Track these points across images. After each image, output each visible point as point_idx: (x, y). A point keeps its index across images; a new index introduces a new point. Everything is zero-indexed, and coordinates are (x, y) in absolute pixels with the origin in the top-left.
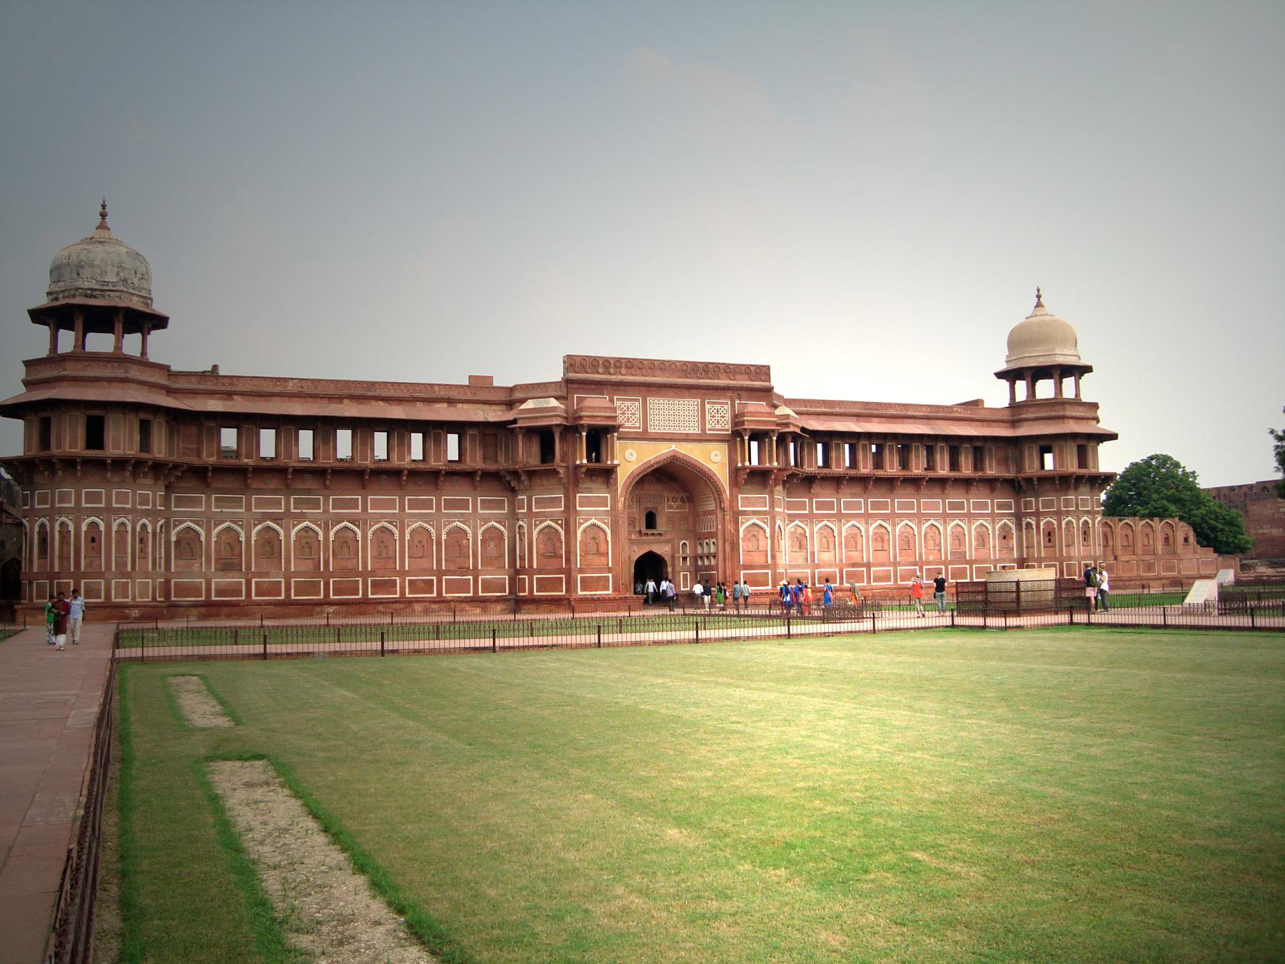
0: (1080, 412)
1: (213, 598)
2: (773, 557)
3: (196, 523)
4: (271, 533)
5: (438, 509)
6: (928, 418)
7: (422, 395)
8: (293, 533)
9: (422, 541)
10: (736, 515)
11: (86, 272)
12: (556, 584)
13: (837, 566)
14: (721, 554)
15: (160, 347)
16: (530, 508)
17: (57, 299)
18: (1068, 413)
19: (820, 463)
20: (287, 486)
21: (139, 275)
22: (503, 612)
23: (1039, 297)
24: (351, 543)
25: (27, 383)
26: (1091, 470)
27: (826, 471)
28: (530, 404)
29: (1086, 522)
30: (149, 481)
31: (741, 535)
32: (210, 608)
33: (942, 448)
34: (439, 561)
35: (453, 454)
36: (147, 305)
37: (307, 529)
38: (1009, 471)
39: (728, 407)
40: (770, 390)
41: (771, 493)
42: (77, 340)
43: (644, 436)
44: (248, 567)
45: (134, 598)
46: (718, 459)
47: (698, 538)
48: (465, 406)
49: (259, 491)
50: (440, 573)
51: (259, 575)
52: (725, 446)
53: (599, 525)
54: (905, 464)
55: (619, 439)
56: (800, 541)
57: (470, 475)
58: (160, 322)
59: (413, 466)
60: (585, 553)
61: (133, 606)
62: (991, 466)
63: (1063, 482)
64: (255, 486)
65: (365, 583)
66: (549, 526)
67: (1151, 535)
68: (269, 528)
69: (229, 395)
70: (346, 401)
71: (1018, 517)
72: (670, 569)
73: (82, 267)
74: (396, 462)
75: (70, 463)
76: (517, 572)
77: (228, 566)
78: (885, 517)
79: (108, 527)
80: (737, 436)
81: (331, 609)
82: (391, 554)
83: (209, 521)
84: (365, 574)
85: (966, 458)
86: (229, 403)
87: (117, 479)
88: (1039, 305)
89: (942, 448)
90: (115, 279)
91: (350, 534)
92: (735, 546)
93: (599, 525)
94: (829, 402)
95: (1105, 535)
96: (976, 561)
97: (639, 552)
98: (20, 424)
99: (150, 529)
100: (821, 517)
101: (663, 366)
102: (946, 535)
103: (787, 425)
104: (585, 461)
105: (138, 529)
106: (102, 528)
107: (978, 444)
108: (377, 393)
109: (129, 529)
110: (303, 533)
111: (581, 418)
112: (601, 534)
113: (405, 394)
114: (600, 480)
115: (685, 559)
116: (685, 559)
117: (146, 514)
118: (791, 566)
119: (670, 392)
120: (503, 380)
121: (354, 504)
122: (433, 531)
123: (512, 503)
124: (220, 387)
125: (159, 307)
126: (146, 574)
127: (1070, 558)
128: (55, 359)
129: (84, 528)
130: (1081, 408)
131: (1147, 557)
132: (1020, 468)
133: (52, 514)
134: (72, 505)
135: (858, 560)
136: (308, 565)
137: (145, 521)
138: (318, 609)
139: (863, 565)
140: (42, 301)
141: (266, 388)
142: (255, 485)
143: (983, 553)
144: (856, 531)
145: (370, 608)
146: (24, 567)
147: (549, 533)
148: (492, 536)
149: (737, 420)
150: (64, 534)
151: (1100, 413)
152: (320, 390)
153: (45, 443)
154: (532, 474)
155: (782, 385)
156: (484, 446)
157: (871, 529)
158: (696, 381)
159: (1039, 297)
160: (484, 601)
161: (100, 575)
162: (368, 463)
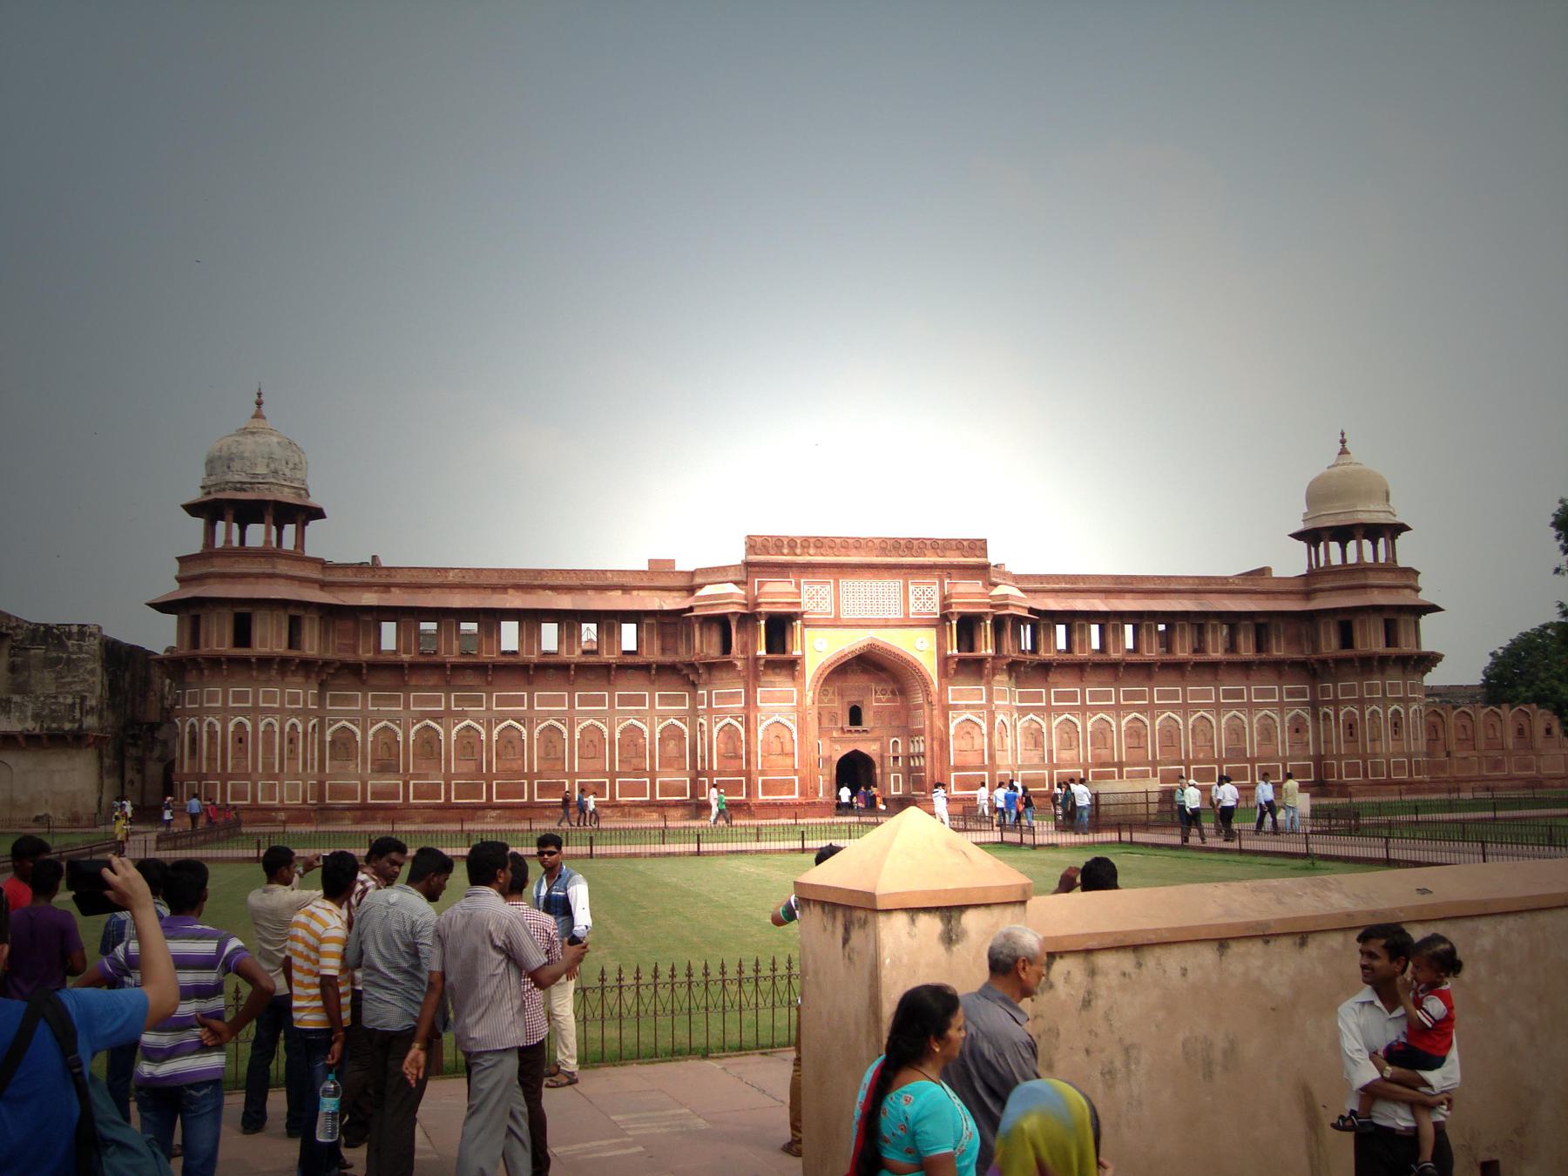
0: (1388, 579)
2: (992, 757)
3: (351, 721)
5: (612, 705)
7: (594, 583)
9: (593, 741)
10: (946, 709)
11: (236, 465)
13: (1080, 765)
14: (928, 754)
15: (321, 541)
16: (710, 703)
18: (1371, 581)
20: (448, 683)
22: (683, 818)
23: (1343, 442)
24: (516, 742)
25: (182, 580)
26: (1406, 648)
29: (1397, 712)
30: (299, 679)
31: (952, 732)
33: (1182, 628)
37: (469, 727)
38: (1302, 652)
39: (936, 588)
41: (989, 683)
43: (836, 623)
44: (406, 768)
45: (282, 801)
47: (911, 734)
48: (642, 593)
49: (417, 688)
50: (613, 775)
51: (417, 776)
52: (932, 632)
53: (786, 725)
56: (1036, 738)
57: (645, 668)
58: (318, 514)
59: (583, 659)
60: (768, 753)
64: (413, 682)
67: (1498, 726)
68: (428, 726)
69: (387, 587)
70: (511, 591)
71: (1314, 706)
72: (878, 771)
73: (231, 459)
74: (565, 656)
75: (215, 662)
76: (699, 774)
77: (385, 766)
79: (255, 727)
81: (494, 813)
83: (365, 720)
84: (531, 776)
85: (1246, 637)
87: (263, 677)
88: (1344, 452)
92: (944, 745)
93: (786, 725)
96: (1259, 759)
97: (841, 751)
98: (172, 619)
99: (300, 729)
100: (1095, 710)
101: (846, 544)
102: (1219, 728)
103: (1006, 606)
104: (762, 652)
105: (287, 729)
106: (249, 728)
107: (1261, 621)
108: (545, 581)
109: (277, 729)
110: (464, 733)
111: (758, 605)
113: (575, 582)
114: (784, 672)
115: (896, 759)
116: (896, 759)
117: (296, 713)
118: (1020, 768)
119: (867, 572)
123: (693, 698)
125: (315, 500)
126: (296, 776)
127: (1375, 755)
129: (231, 728)
130: (1389, 575)
131: (1491, 753)
132: (1316, 649)
133: (200, 713)
136: (470, 767)
137: (294, 720)
138: (480, 813)
139: (1114, 765)
140: (196, 495)
145: (536, 811)
146: (177, 769)
147: (729, 732)
148: (672, 734)
149: (945, 604)
152: (483, 580)
153: (195, 643)
154: (711, 667)
156: (663, 636)
157: (1123, 723)
158: (901, 559)
159: (1343, 442)
160: (662, 806)
161: (247, 776)
162: (535, 658)
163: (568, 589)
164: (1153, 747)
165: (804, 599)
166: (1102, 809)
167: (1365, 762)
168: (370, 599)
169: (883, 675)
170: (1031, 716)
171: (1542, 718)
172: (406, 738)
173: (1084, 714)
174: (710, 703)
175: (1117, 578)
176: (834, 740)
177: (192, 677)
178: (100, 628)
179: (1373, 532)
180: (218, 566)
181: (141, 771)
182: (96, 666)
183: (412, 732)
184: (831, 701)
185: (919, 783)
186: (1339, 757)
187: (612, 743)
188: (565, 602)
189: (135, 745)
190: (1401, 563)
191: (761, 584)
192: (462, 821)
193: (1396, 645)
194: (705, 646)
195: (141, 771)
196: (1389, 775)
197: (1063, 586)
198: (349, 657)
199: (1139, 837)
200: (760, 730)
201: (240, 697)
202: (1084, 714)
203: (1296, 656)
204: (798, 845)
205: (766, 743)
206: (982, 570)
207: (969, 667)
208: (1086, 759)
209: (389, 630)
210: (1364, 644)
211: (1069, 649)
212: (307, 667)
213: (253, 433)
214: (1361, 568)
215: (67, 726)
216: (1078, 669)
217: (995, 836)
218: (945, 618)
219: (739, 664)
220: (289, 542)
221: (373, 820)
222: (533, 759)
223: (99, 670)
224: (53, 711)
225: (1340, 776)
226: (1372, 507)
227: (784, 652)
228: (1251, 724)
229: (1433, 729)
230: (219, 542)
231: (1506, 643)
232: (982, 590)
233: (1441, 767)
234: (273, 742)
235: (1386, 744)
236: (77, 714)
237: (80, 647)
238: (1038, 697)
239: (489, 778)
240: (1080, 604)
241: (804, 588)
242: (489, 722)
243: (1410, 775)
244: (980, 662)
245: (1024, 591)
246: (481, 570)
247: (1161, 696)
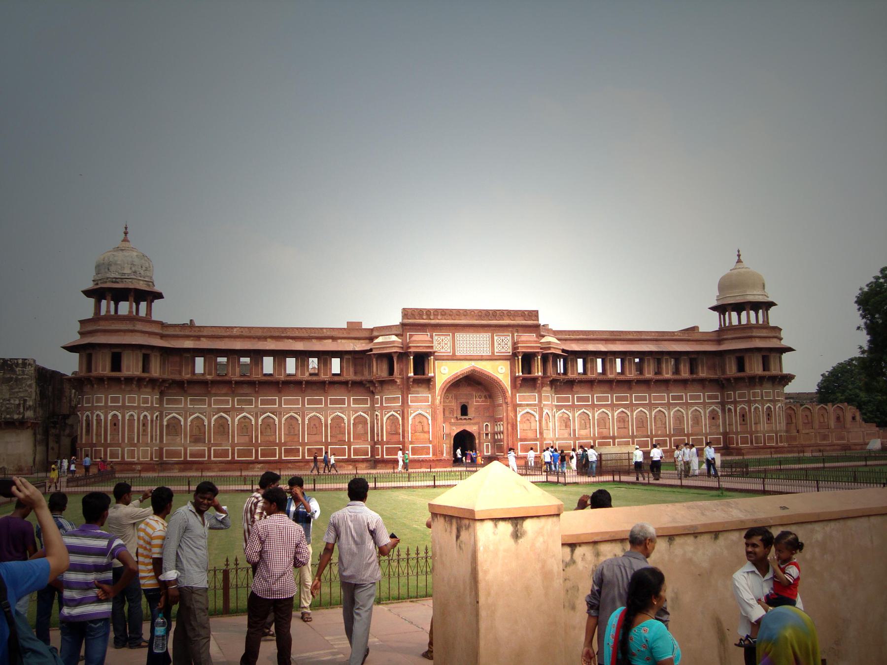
0: (764, 333)
1: (188, 459)
2: (541, 433)
3: (178, 414)
6: (656, 340)
7: (316, 335)
8: (236, 420)
10: (515, 406)
11: (113, 268)
13: (591, 438)
14: (505, 432)
15: (161, 311)
16: (382, 403)
18: (754, 334)
20: (233, 392)
22: (367, 468)
23: (739, 256)
25: (81, 333)
26: (774, 371)
27: (584, 377)
29: (769, 408)
30: (149, 390)
31: (519, 419)
33: (649, 360)
34: (326, 436)
36: (149, 285)
37: (245, 417)
38: (716, 374)
39: (509, 338)
40: (537, 326)
43: (453, 358)
44: (210, 440)
45: (138, 459)
46: (503, 371)
48: (343, 341)
49: (216, 395)
50: (327, 444)
51: (215, 445)
52: (508, 363)
53: (425, 416)
55: (435, 359)
56: (566, 422)
57: (345, 383)
58: (159, 296)
59: (310, 378)
60: (415, 431)
61: (136, 464)
62: (703, 370)
64: (213, 392)
67: (826, 416)
68: (221, 416)
69: (198, 338)
70: (269, 340)
71: (723, 404)
72: (477, 441)
74: (300, 377)
75: (101, 380)
76: (375, 443)
77: (197, 439)
78: (625, 406)
81: (260, 466)
82: (296, 432)
83: (186, 413)
84: (280, 445)
85: (685, 366)
87: (128, 389)
88: (739, 261)
89: (667, 360)
90: (129, 272)
92: (514, 426)
93: (425, 416)
96: (692, 435)
97: (456, 430)
98: (76, 356)
99: (149, 418)
101: (459, 313)
103: (549, 348)
104: (411, 374)
105: (142, 418)
106: (120, 418)
108: (289, 334)
109: (136, 418)
111: (410, 347)
112: (425, 419)
115: (487, 434)
116: (487, 434)
117: (147, 409)
118: (557, 439)
121: (273, 402)
124: (192, 333)
125: (157, 288)
126: (147, 445)
127: (757, 432)
128: (97, 318)
130: (764, 331)
131: (822, 431)
132: (723, 371)
133: (92, 409)
134: (103, 404)
137: (145, 413)
138: (251, 466)
139: (610, 438)
140: (90, 285)
144: (605, 415)
146: (79, 441)
148: (360, 421)
150: (99, 421)
151: (783, 334)
152: (253, 334)
153: (89, 369)
154: (382, 383)
156: (355, 365)
157: (616, 414)
159: (739, 256)
160: (355, 461)
161: (119, 445)
162: (282, 377)
164: (632, 428)
165: (435, 344)
166: (604, 463)
167: (751, 436)
168: (189, 344)
169: (480, 387)
170: (563, 410)
171: (850, 411)
172: (209, 423)
174: (382, 403)
175: (612, 332)
176: (452, 424)
177: (87, 388)
178: (34, 361)
179: (756, 306)
180: (103, 325)
181: (58, 441)
182: (33, 382)
184: (450, 402)
185: (500, 448)
186: (737, 433)
188: (299, 346)
189: (55, 427)
190: (772, 323)
191: (411, 336)
192: (241, 470)
193: (768, 370)
195: (58, 441)
196: (765, 443)
197: (581, 337)
198: (177, 377)
199: (624, 478)
200: (410, 418)
201: (115, 400)
204: (432, 483)
207: (528, 383)
208: (594, 434)
209: (199, 362)
210: (751, 369)
211: (585, 372)
212: (153, 383)
213: (122, 250)
214: (749, 327)
215: (16, 417)
216: (591, 384)
217: (543, 478)
218: (515, 355)
220: (143, 312)
221: (190, 469)
222: (282, 436)
223: (34, 385)
224: (8, 408)
225: (737, 444)
226: (755, 293)
227: (424, 374)
228: (687, 414)
229: (790, 419)
230: (103, 312)
231: (830, 369)
232: (536, 339)
233: (795, 438)
235: (763, 426)
236: (22, 410)
237: (23, 371)
238: (567, 400)
239: (257, 445)
240: (591, 347)
241: (435, 338)
242: (257, 414)
243: (777, 443)
244: (535, 380)
245: (559, 340)
246: (253, 328)
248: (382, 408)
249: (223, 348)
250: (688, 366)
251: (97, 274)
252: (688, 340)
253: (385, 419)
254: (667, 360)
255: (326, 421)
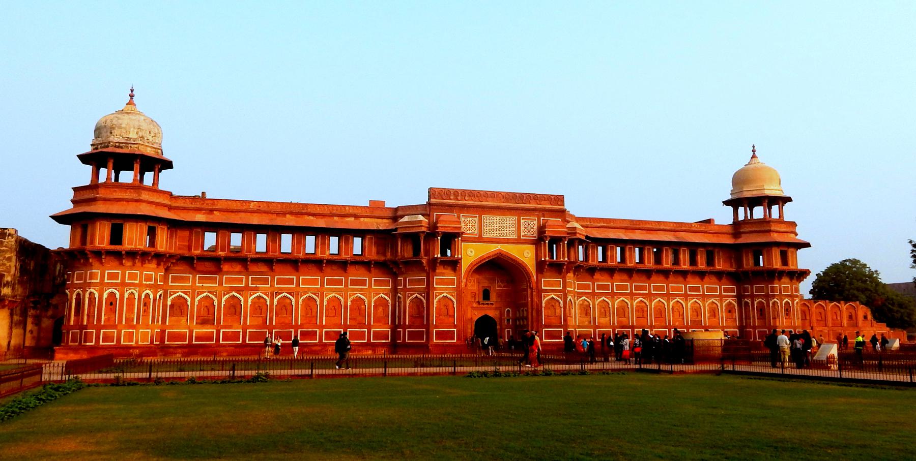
0: (782, 228)
2: (565, 320)
3: (185, 293)
4: (236, 300)
5: (346, 285)
8: (250, 300)
10: (540, 292)
11: (116, 132)
12: (419, 335)
15: (167, 181)
16: (405, 285)
17: (97, 149)
18: (772, 229)
19: (600, 259)
20: (247, 269)
21: (152, 134)
23: (754, 151)
24: (289, 308)
26: (792, 267)
27: (604, 264)
28: (406, 219)
29: (787, 303)
30: (153, 265)
32: (191, 349)
34: (346, 319)
35: (357, 250)
37: (259, 297)
42: (109, 174)
43: (480, 239)
45: (137, 342)
46: (529, 256)
48: (366, 220)
49: (228, 273)
50: (346, 327)
54: (658, 260)
55: (462, 241)
56: (586, 310)
58: (168, 165)
60: (439, 313)
62: (719, 262)
63: (772, 275)
65: (296, 332)
66: (416, 297)
68: (234, 296)
70: (288, 216)
71: (739, 298)
72: (498, 327)
73: (114, 128)
74: (319, 255)
79: (122, 296)
80: (538, 242)
83: (193, 293)
84: (296, 327)
85: (701, 257)
86: (211, 216)
91: (288, 301)
94: (606, 219)
95: (803, 313)
97: (478, 315)
98: (67, 228)
99: (151, 297)
106: (118, 296)
109: (136, 297)
110: (256, 300)
111: (437, 228)
112: (451, 304)
113: (327, 212)
116: (508, 320)
117: (150, 287)
118: (579, 327)
120: (392, 203)
121: (290, 282)
122: (342, 299)
123: (396, 283)
124: (204, 206)
125: (167, 156)
128: (94, 186)
131: (835, 328)
133: (85, 286)
134: (98, 281)
135: (625, 324)
140: (88, 149)
141: (234, 206)
142: (226, 267)
143: (714, 320)
147: (417, 302)
148: (381, 303)
149: (541, 230)
151: (798, 230)
155: (573, 207)
156: (377, 244)
159: (754, 151)
161: (115, 327)
162: (301, 255)
163: (323, 216)
165: (463, 225)
168: (200, 217)
171: (862, 310)
173: (613, 297)
178: (16, 231)
180: (102, 193)
183: (224, 299)
186: (755, 327)
187: (346, 307)
188: (321, 223)
190: (787, 218)
194: (405, 251)
197: (602, 224)
198: (186, 253)
201: (111, 276)
202: (613, 297)
203: (730, 269)
205: (438, 309)
206: (562, 213)
212: (159, 257)
213: (127, 113)
216: (611, 272)
219: (424, 262)
221: (195, 353)
228: (704, 307)
230: (102, 178)
232: (562, 224)
234: (133, 305)
238: (587, 287)
239: (270, 328)
240: (612, 235)
241: (462, 219)
247: (656, 288)
248: (405, 289)
249: (240, 222)
250: (704, 257)
251: (97, 137)
252: (706, 232)
253: (408, 302)
254: (684, 251)
255: (346, 303)
